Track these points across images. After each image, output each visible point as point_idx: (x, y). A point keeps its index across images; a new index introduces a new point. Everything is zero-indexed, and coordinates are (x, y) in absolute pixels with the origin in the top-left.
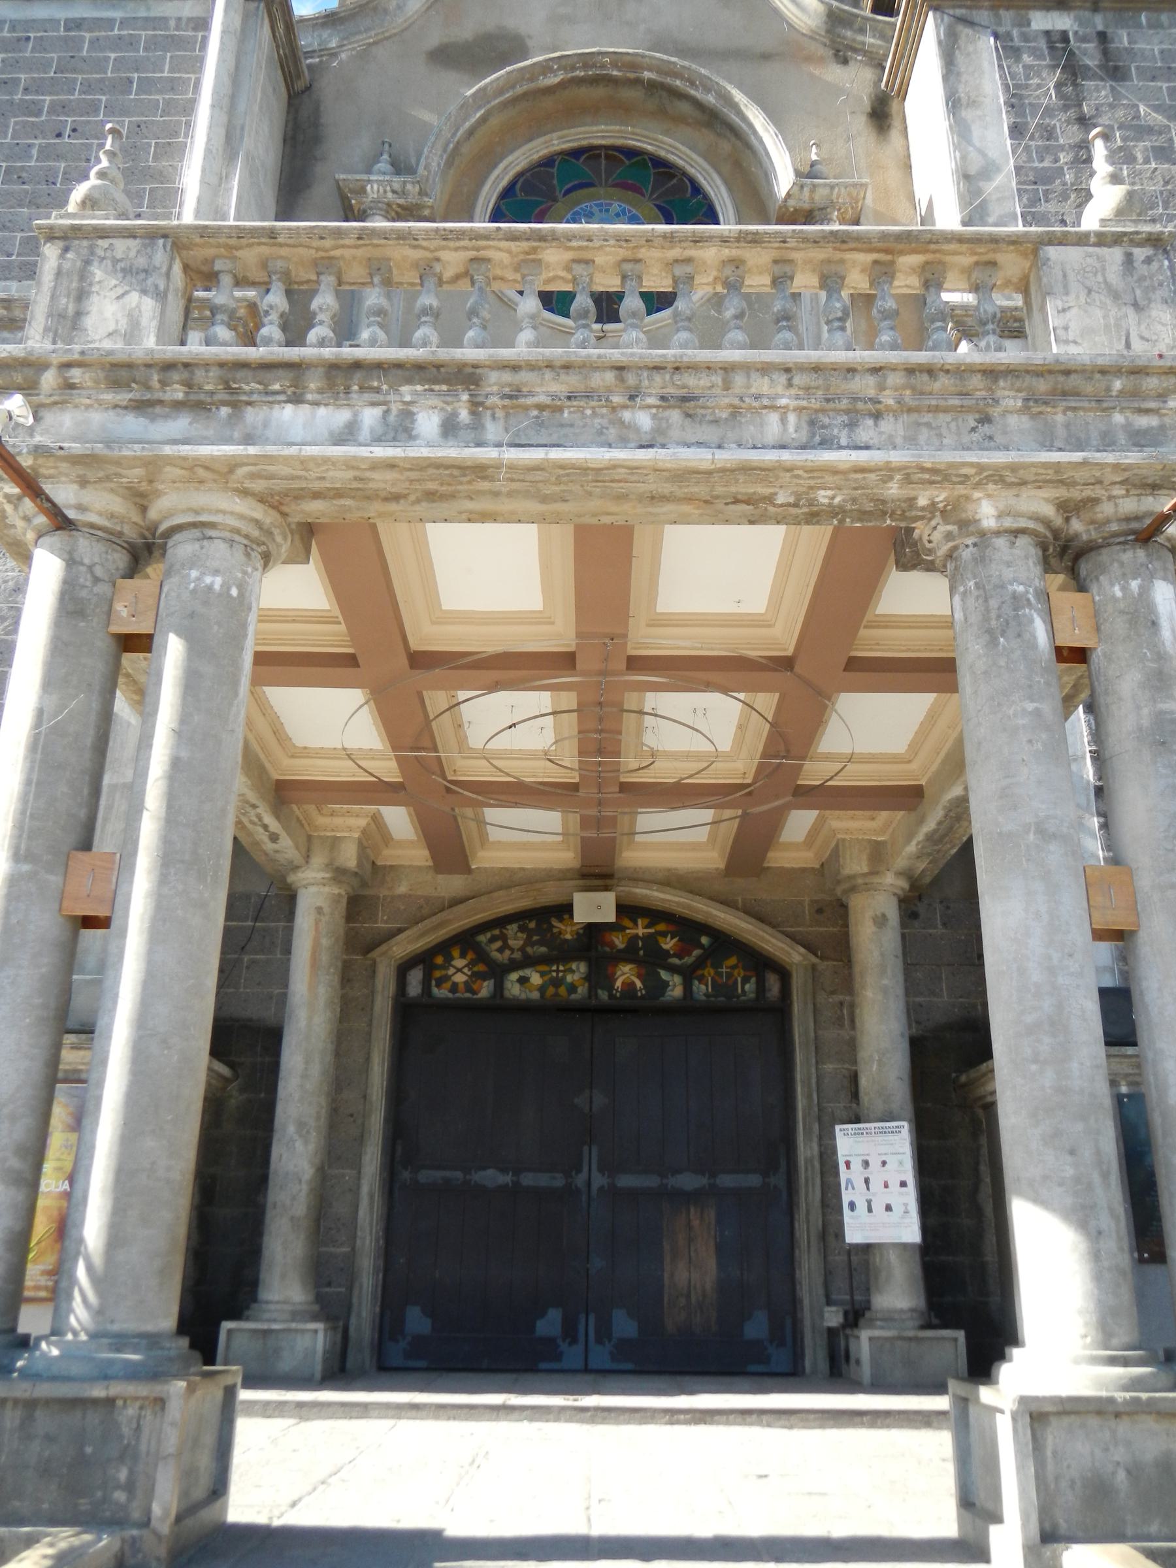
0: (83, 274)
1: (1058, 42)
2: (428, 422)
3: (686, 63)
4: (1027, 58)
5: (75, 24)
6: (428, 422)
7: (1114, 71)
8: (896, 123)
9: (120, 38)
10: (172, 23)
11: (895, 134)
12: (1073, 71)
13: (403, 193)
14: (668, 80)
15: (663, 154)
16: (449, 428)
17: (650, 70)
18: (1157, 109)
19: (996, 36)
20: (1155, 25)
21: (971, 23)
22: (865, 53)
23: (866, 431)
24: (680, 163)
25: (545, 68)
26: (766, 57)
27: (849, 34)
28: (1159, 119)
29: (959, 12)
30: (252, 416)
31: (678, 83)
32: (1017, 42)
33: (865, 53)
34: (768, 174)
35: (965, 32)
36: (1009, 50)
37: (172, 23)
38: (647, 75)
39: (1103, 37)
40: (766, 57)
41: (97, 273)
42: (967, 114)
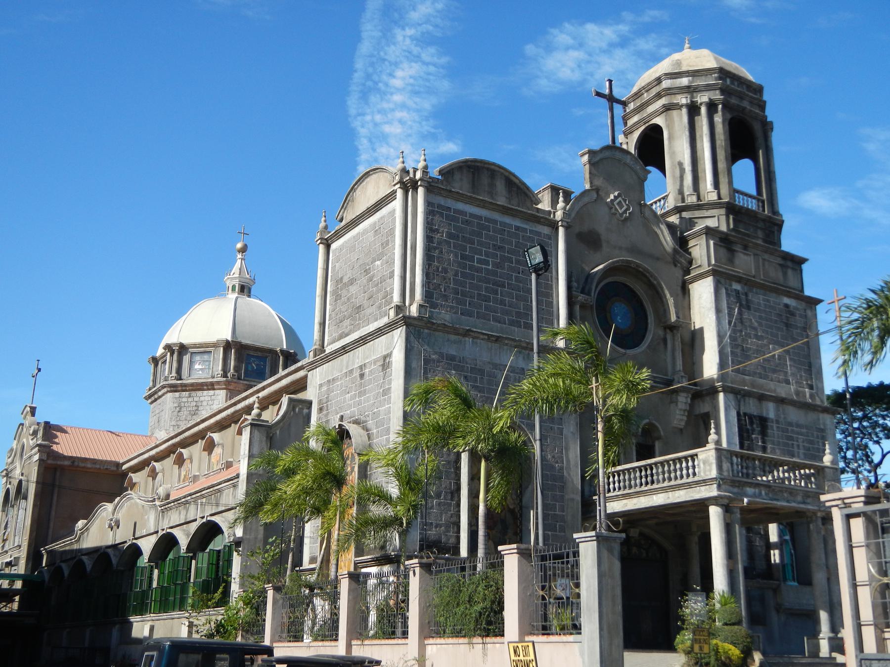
0: (721, 458)
1: (737, 292)
2: (763, 492)
3: (652, 271)
4: (732, 299)
5: (517, 228)
6: (763, 492)
7: (749, 308)
8: (687, 291)
9: (530, 237)
10: (543, 235)
11: (687, 296)
12: (741, 306)
13: (587, 300)
14: (645, 273)
15: (635, 289)
16: (766, 494)
17: (642, 268)
18: (756, 321)
19: (726, 289)
20: (757, 293)
21: (721, 283)
22: (681, 264)
23: (809, 500)
24: (639, 294)
25: (617, 262)
26: (658, 259)
27: (678, 257)
28: (756, 324)
29: (718, 278)
30: (744, 488)
31: (647, 274)
32: (729, 292)
33: (681, 264)
34: (666, 311)
35: (720, 285)
36: (728, 295)
37: (543, 235)
38: (640, 269)
39: (746, 294)
40: (658, 259)
41: (723, 458)
42: (721, 315)
